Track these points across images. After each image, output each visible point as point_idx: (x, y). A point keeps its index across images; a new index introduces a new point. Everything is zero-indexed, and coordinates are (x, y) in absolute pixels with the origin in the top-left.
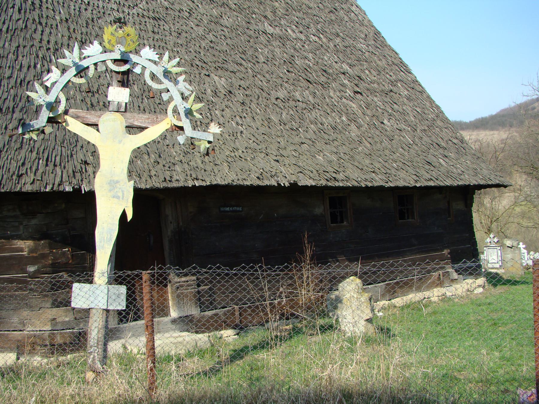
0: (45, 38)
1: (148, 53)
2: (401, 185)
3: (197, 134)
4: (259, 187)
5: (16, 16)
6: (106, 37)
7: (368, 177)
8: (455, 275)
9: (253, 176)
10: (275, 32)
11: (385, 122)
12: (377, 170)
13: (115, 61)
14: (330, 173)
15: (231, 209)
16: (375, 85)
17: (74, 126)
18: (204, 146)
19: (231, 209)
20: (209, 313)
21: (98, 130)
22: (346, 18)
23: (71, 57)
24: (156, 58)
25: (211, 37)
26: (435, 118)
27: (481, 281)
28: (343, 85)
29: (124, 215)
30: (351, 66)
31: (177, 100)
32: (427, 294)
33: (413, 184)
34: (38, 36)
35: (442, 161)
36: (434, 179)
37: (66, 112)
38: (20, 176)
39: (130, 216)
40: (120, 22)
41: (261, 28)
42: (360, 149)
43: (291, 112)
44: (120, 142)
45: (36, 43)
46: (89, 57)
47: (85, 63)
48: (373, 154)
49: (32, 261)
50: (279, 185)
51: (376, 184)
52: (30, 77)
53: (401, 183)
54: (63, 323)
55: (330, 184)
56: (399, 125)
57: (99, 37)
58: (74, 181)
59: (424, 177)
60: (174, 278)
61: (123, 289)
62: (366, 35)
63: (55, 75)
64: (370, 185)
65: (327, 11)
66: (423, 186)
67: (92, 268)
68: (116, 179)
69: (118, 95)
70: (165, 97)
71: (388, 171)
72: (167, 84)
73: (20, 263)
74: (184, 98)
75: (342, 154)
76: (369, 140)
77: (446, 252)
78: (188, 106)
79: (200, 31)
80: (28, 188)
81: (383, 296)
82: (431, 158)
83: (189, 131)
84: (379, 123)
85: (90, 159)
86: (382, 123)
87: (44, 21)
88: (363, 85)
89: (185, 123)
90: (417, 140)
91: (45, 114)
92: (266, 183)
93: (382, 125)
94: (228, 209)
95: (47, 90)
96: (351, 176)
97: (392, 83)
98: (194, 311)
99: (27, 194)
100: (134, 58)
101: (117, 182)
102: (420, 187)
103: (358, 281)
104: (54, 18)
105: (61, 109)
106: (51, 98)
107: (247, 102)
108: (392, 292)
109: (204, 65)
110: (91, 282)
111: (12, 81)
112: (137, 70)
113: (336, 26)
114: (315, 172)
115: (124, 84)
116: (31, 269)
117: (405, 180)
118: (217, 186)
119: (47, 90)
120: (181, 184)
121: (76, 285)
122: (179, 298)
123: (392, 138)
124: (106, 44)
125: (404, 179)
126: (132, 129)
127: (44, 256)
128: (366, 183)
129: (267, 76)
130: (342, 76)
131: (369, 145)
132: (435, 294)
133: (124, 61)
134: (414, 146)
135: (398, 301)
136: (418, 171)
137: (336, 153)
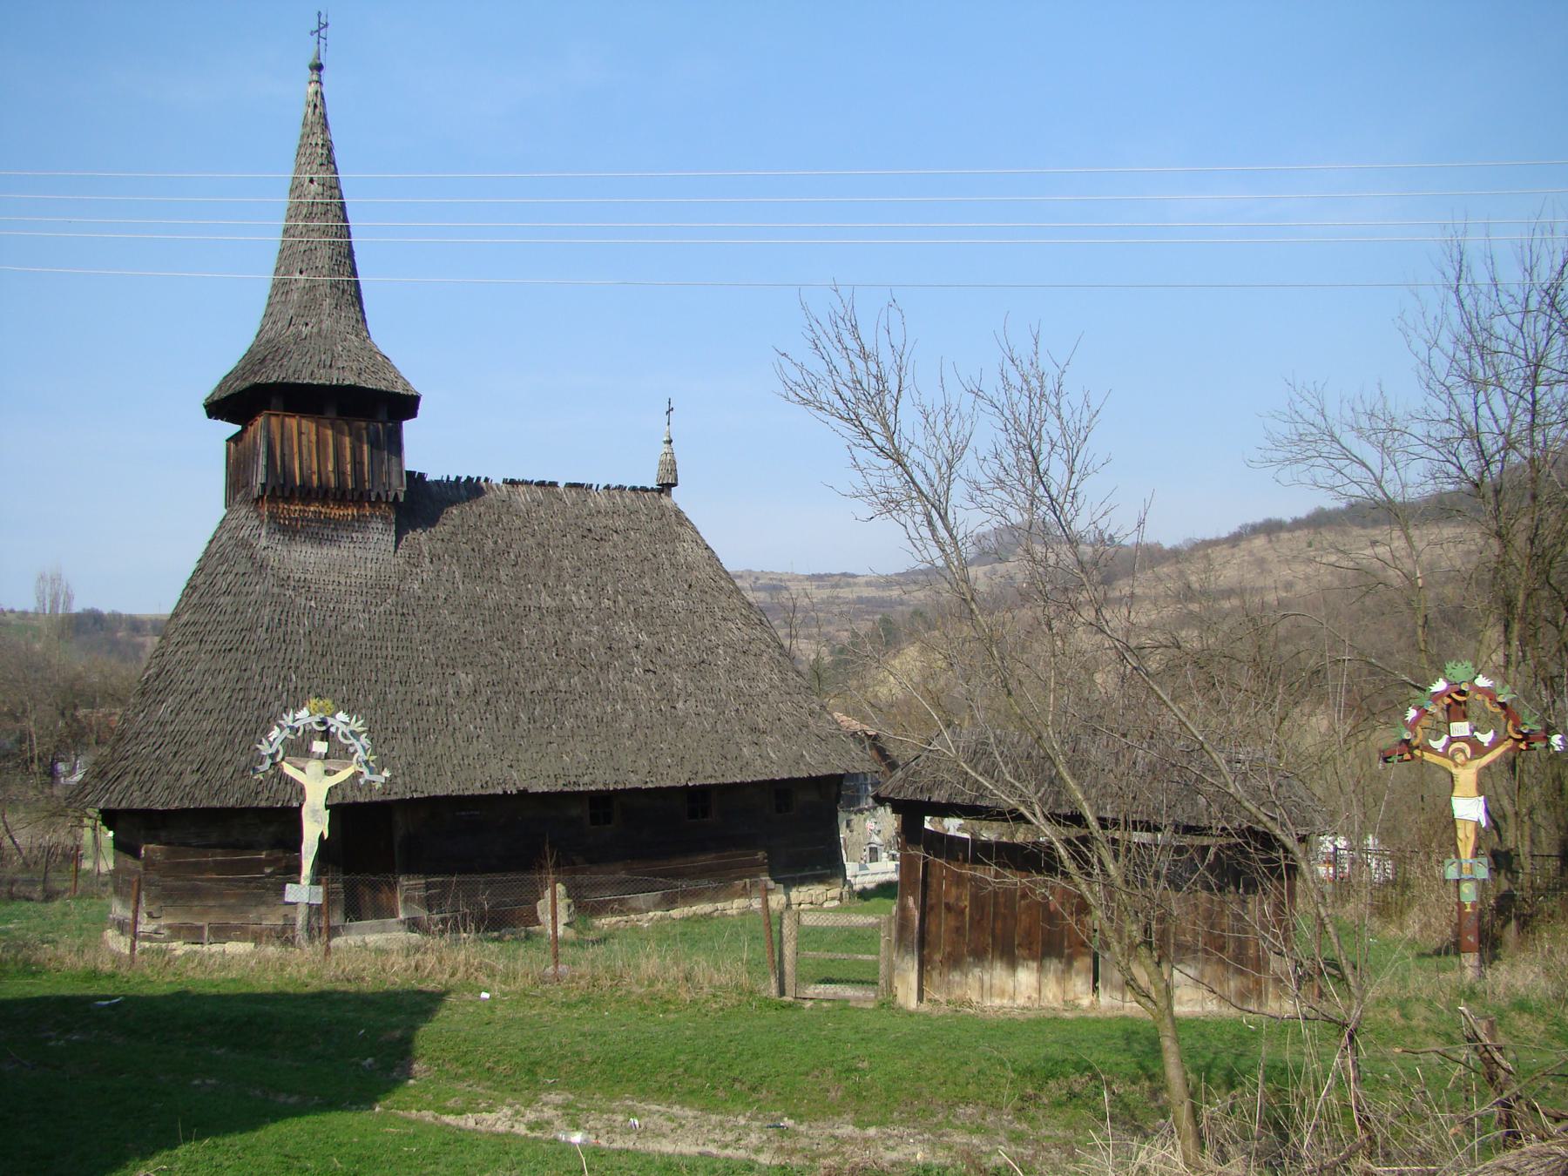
1: (341, 716)
3: (373, 778)
4: (481, 796)
5: (263, 636)
7: (620, 779)
8: (771, 884)
9: (478, 784)
11: (680, 705)
13: (319, 723)
17: (289, 769)
18: (378, 786)
23: (288, 720)
27: (835, 892)
28: (633, 664)
30: (650, 634)
31: (360, 752)
32: (720, 905)
33: (683, 783)
43: (547, 706)
45: (279, 664)
47: (296, 725)
49: (268, 863)
51: (628, 786)
52: (271, 699)
60: (403, 881)
61: (321, 889)
64: (620, 787)
67: (299, 873)
69: (320, 747)
70: (351, 750)
72: (353, 741)
73: (260, 865)
74: (366, 751)
77: (761, 855)
80: (263, 804)
81: (657, 907)
85: (301, 791)
91: (268, 762)
92: (490, 791)
97: (711, 650)
100: (330, 721)
108: (669, 902)
110: (298, 882)
112: (333, 729)
116: (268, 870)
126: (328, 773)
132: (735, 906)
133: (323, 722)
135: (676, 913)
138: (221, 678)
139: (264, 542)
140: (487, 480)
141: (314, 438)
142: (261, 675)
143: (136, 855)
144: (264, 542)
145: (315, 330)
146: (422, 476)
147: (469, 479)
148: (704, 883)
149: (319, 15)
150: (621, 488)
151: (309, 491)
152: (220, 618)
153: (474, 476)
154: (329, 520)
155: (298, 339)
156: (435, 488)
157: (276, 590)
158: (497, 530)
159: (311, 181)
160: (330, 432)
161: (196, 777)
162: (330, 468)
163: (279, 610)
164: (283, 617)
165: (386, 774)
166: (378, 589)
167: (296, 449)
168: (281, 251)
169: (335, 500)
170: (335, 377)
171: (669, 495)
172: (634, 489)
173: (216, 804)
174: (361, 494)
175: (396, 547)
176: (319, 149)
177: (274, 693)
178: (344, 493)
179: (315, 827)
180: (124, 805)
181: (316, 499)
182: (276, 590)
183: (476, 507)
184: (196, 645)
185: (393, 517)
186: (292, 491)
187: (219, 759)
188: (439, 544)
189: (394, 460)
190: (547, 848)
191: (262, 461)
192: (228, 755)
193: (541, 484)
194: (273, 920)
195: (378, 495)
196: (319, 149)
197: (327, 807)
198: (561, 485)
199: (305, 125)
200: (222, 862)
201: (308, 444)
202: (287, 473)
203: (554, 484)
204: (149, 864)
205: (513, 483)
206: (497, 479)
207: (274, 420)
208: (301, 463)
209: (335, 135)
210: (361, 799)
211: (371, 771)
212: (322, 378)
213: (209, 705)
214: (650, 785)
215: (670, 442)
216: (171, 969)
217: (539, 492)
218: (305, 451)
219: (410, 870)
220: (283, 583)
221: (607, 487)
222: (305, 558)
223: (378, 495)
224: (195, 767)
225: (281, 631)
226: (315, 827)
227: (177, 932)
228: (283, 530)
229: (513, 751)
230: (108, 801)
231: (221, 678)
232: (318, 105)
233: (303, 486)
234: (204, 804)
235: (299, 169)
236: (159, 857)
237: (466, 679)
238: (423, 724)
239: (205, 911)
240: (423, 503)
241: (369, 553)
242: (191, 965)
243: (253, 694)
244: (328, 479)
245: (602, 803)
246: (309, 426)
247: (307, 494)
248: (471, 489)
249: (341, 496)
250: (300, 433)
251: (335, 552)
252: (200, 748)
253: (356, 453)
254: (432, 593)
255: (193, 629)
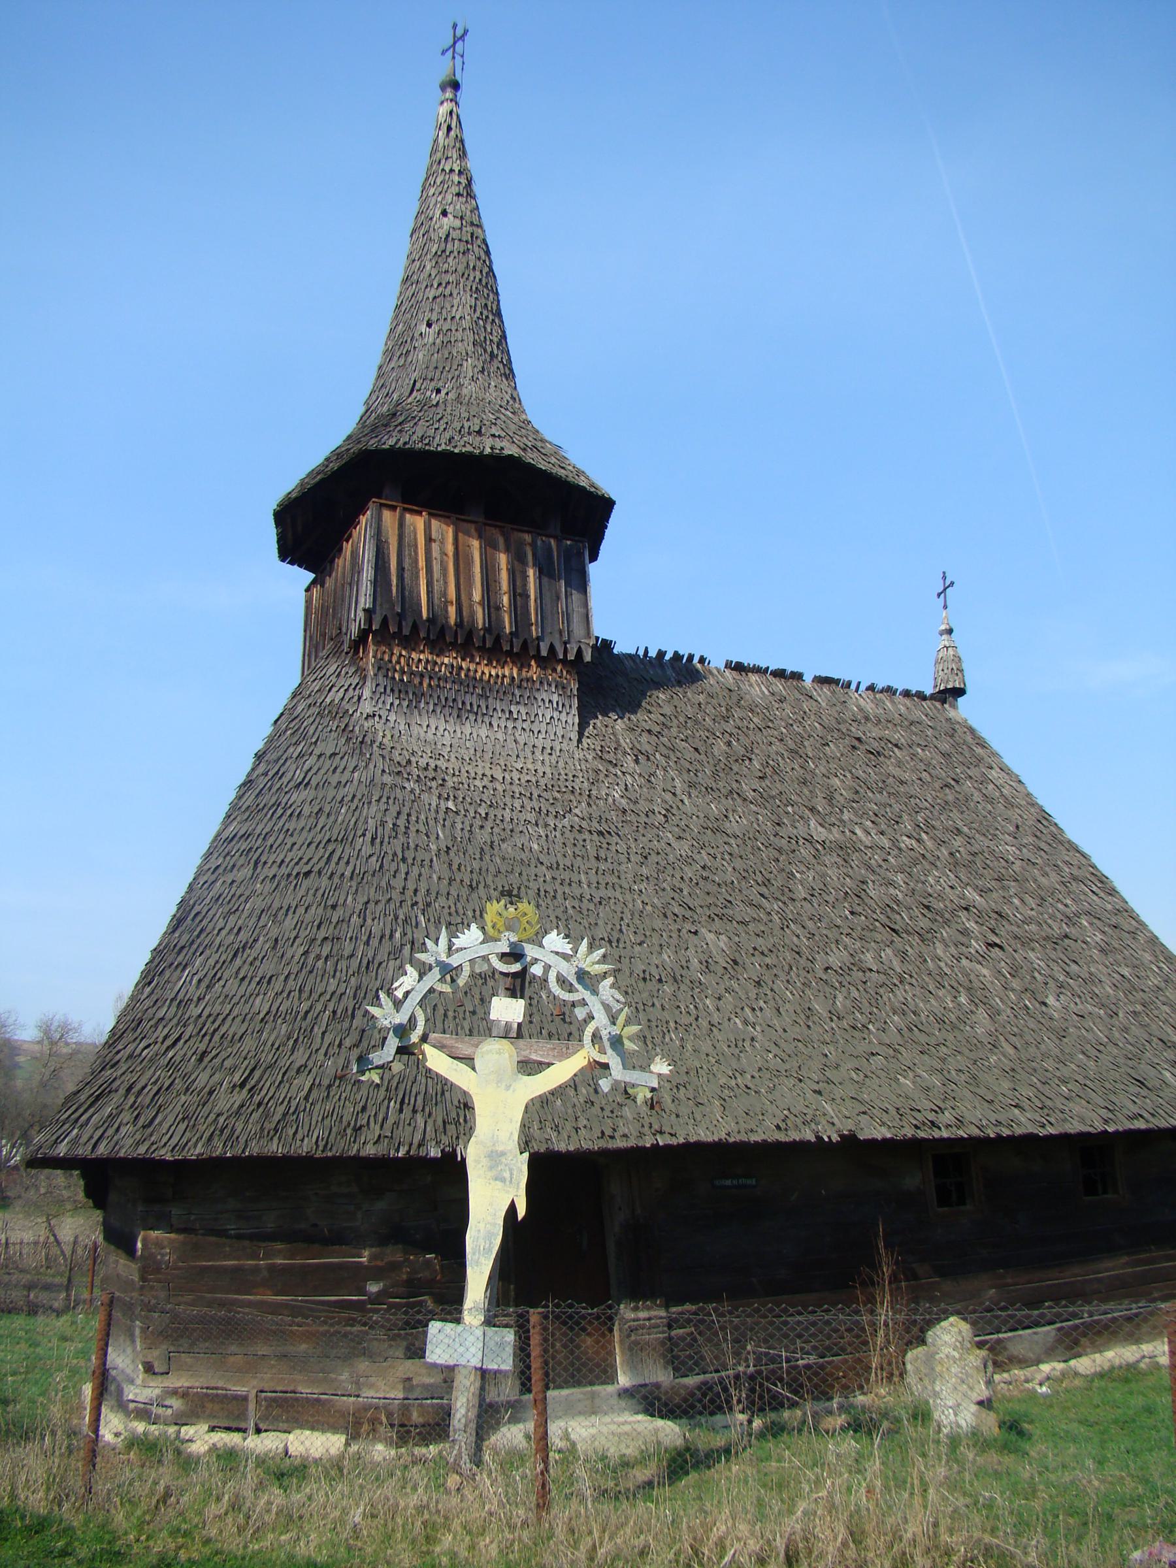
0: (411, 886)
1: (555, 941)
2: (1072, 1132)
4: (778, 1144)
5: (367, 850)
6: (488, 918)
7: (1002, 1117)
9: (769, 1123)
10: (831, 837)
11: (1051, 1000)
12: (1025, 1104)
13: (503, 956)
14: (924, 1112)
15: (735, 1182)
16: (1033, 927)
17: (437, 1061)
18: (643, 1095)
19: (735, 1182)
20: (691, 1381)
21: (474, 1069)
22: (977, 796)
23: (436, 951)
24: (567, 948)
25: (704, 858)
26: (1163, 985)
28: (965, 932)
29: (512, 1208)
30: (982, 892)
31: (601, 1019)
33: (1099, 1126)
34: (398, 883)
35: (1168, 1074)
36: (1146, 1115)
37: (424, 1038)
38: (357, 1130)
39: (521, 1212)
40: (510, 895)
41: (801, 830)
42: (993, 1059)
44: (508, 1088)
46: (462, 949)
47: (455, 961)
48: (1020, 1070)
49: (375, 1273)
50: (819, 1138)
51: (1019, 1131)
52: (382, 955)
53: (1074, 1127)
54: (426, 1387)
55: (922, 1134)
56: (1080, 1006)
57: (479, 916)
58: (445, 1140)
59: (1125, 1111)
60: (627, 1312)
61: (509, 1336)
62: (1017, 827)
63: (408, 981)
64: (1006, 1132)
65: (937, 785)
66: (1121, 1129)
68: (500, 1148)
69: (507, 1010)
70: (580, 1013)
71: (1048, 1103)
72: (582, 993)
73: (356, 1277)
75: (953, 1072)
76: (1013, 1039)
78: (616, 1030)
79: (683, 848)
80: (370, 1150)
81: (1049, 1353)
82: (1145, 1070)
83: (618, 1071)
84: (1038, 1005)
86: (1045, 1004)
87: (410, 855)
88: (1005, 929)
89: (611, 1058)
90: (1117, 1035)
91: (393, 1043)
92: (794, 1136)
93: (1044, 1008)
94: (728, 1182)
95: (398, 1004)
96: (968, 1116)
97: (1069, 920)
98: (662, 1376)
99: (367, 1160)
100: (531, 951)
101: (503, 1154)
102: (1117, 1132)
103: (965, 1327)
104: (427, 849)
105: (415, 1037)
106: (401, 1018)
107: (767, 978)
108: (1071, 1343)
109: (688, 913)
110: (458, 1321)
111: (355, 963)
113: (955, 814)
114: (893, 1111)
115: (513, 993)
116: (373, 1288)
117: (1082, 1120)
118: (699, 1145)
119: (398, 1004)
120: (631, 1143)
121: (434, 1327)
122: (635, 1350)
123: (1063, 1034)
124: (489, 928)
125: (1083, 1118)
126: (529, 1067)
127: (394, 1267)
128: (997, 1130)
129: (810, 924)
130: (963, 915)
131: (1011, 1051)
133: (515, 955)
134: (1110, 1048)
135: (1085, 1364)
136: (1113, 1098)
137: (941, 1071)
138: (289, 922)
139: (367, 707)
140: (702, 660)
141: (450, 549)
142: (362, 914)
143: (130, 1251)
144: (367, 707)
145: (452, 396)
146: (607, 645)
147: (677, 657)
148: (1117, 1310)
149: (455, 26)
150: (890, 691)
151: (443, 630)
152: (291, 826)
153: (684, 652)
154: (471, 683)
155: (424, 405)
156: (628, 664)
157: (387, 779)
158: (729, 727)
159: (444, 213)
160: (476, 544)
161: (240, 1097)
162: (477, 596)
163: (394, 810)
164: (401, 822)
165: (661, 1067)
166: (554, 796)
167: (422, 563)
168: (398, 307)
169: (482, 649)
170: (487, 446)
171: (954, 707)
172: (907, 694)
173: (275, 1148)
174: (525, 645)
175: (581, 734)
176: (451, 172)
177: (387, 946)
178: (498, 639)
179: (494, 1194)
180: (102, 1150)
181: (454, 646)
182: (387, 779)
183: (692, 694)
184: (247, 872)
185: (574, 686)
186: (415, 627)
187: (284, 1062)
188: (645, 738)
189: (576, 596)
190: (881, 1244)
191: (368, 574)
192: (300, 1057)
193: (780, 674)
194: (382, 1384)
195: (552, 648)
196: (451, 172)
197: (525, 1143)
198: (808, 679)
199: (433, 152)
200: (285, 1269)
201: (438, 558)
202: (407, 599)
203: (797, 676)
204: (150, 1268)
205: (739, 668)
206: (717, 662)
207: (387, 515)
208: (429, 584)
209: (473, 164)
210: (561, 1146)
211: (628, 1063)
212: (464, 445)
213: (268, 968)
214: (1052, 1131)
215: (950, 631)
216: (168, 1514)
217: (779, 685)
218: (436, 568)
219: (638, 1293)
220: (401, 770)
221: (871, 688)
222: (433, 735)
223: (552, 648)
224: (237, 1078)
225: (397, 845)
226: (494, 1194)
227: (199, 1406)
228: (400, 689)
229: (816, 1065)
230: (75, 1142)
231: (289, 922)
232: (452, 125)
233: (432, 620)
234: (254, 1149)
235: (424, 199)
236: (167, 1256)
237: (717, 942)
238: (655, 1013)
239: (251, 1367)
240: (612, 683)
241: (541, 732)
242: (213, 1509)
243: (348, 949)
244: (472, 614)
245: (952, 1163)
246: (444, 531)
247: (439, 636)
248: (681, 671)
249: (494, 647)
250: (429, 540)
251: (484, 732)
252: (249, 1044)
253: (518, 577)
254: (643, 806)
255: (244, 845)
